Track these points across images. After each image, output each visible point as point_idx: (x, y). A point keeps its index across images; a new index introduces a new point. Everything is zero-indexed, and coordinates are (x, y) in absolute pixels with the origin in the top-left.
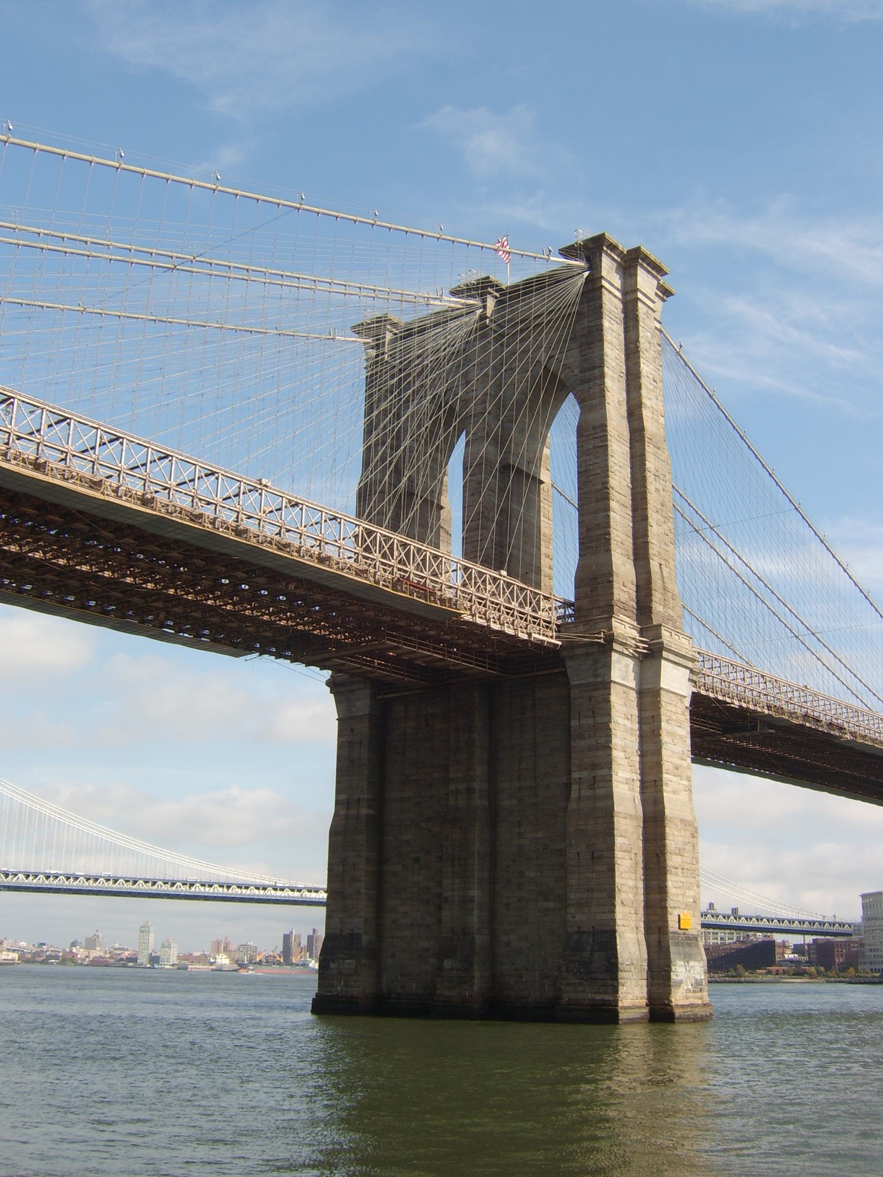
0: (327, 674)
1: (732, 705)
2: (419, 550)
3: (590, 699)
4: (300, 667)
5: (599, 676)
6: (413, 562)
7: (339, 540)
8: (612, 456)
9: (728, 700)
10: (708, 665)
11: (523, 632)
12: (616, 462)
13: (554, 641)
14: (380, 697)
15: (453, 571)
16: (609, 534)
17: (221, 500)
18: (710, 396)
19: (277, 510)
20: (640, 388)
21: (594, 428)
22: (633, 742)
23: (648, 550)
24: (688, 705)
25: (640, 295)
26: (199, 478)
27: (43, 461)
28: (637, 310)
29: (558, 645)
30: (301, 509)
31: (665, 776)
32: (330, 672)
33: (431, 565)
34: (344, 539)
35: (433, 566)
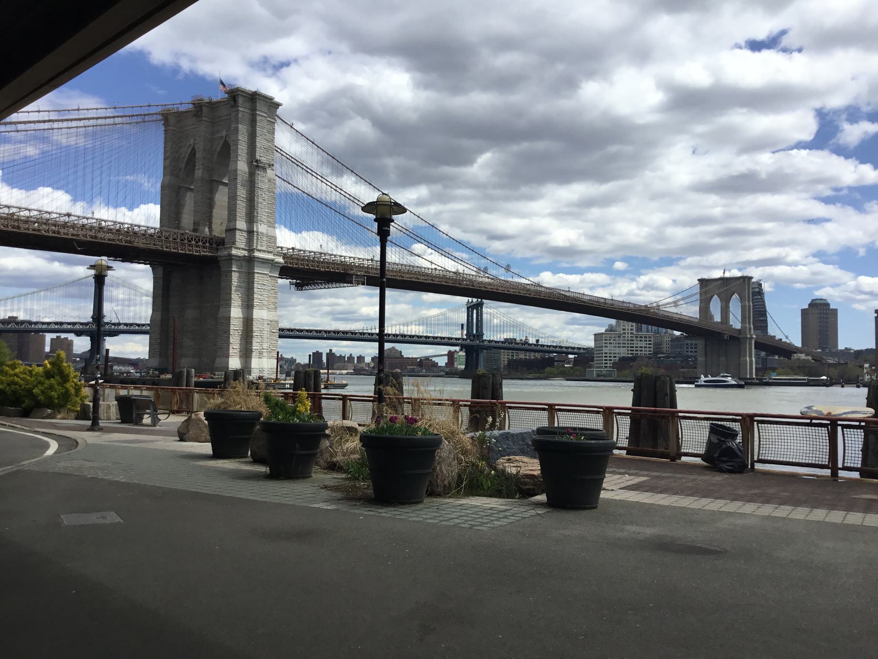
21: (234, 170)
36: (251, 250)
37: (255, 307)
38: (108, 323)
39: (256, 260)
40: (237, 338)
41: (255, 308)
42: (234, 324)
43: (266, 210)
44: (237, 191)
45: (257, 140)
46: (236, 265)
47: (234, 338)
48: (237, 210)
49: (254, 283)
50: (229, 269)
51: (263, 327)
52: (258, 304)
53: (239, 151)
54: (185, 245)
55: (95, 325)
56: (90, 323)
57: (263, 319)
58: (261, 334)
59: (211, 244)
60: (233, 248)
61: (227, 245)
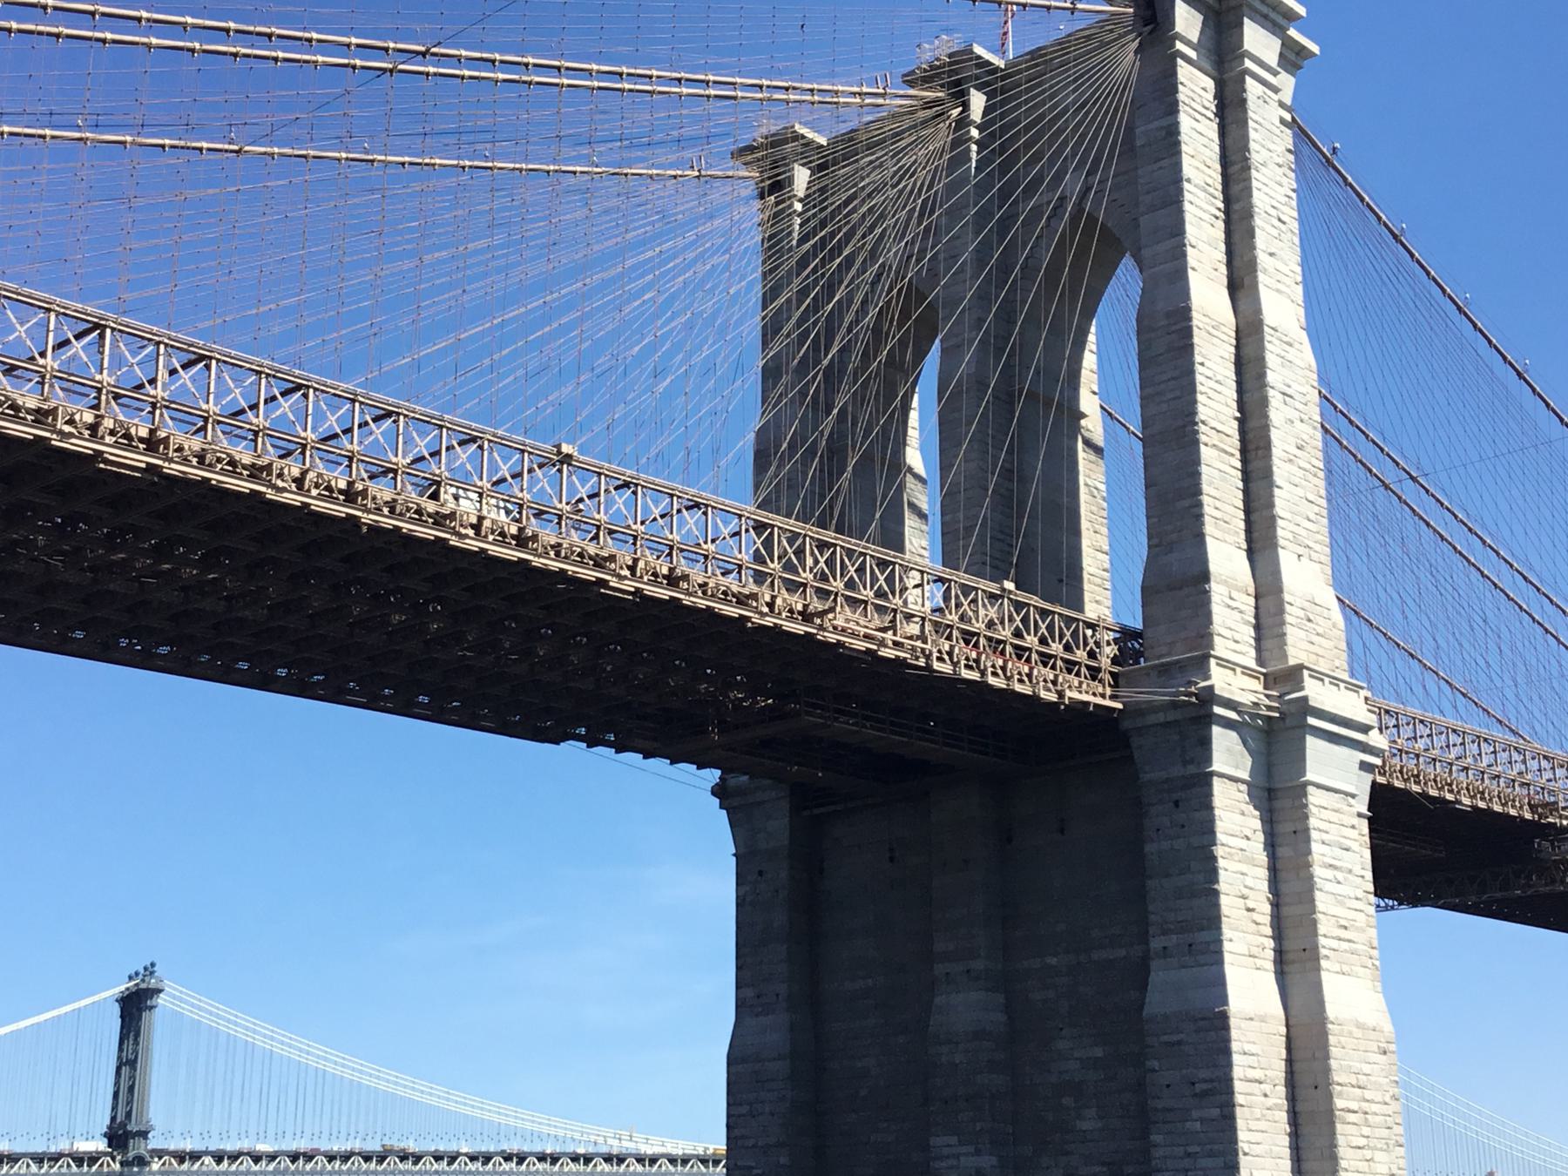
0: (713, 775)
1: (1457, 806)
2: (850, 553)
3: (1176, 804)
4: (659, 764)
5: (1192, 761)
6: (842, 575)
7: (706, 543)
8: (1202, 364)
9: (1450, 797)
10: (1407, 732)
11: (1049, 690)
12: (1210, 374)
13: (1108, 703)
14: (806, 813)
15: (916, 586)
16: (1200, 505)
17: (489, 486)
18: (1395, 237)
19: (590, 497)
20: (1253, 236)
21: (1168, 315)
22: (1258, 878)
23: (1275, 530)
24: (1364, 810)
25: (1248, 64)
26: (448, 449)
27: (164, 435)
28: (1245, 91)
29: (1114, 709)
30: (635, 493)
31: (1322, 941)
32: (717, 773)
33: (874, 579)
34: (713, 541)
35: (878, 580)
36: (1284, 678)
37: (1327, 957)
38: (159, 1154)
39: (1312, 721)
40: (1262, 1125)
41: (1323, 963)
42: (1247, 1047)
43: (1311, 497)
44: (1195, 402)
45: (1255, 184)
46: (1229, 750)
47: (1253, 1125)
48: (1205, 488)
49: (1308, 840)
50: (1192, 769)
51: (1367, 1068)
52: (1334, 944)
53: (1189, 228)
54: (1003, 653)
55: (119, 1158)
56: (105, 1154)
57: (1360, 1026)
58: (1365, 1105)
59: (1092, 655)
60: (1213, 662)
61: (1159, 657)
